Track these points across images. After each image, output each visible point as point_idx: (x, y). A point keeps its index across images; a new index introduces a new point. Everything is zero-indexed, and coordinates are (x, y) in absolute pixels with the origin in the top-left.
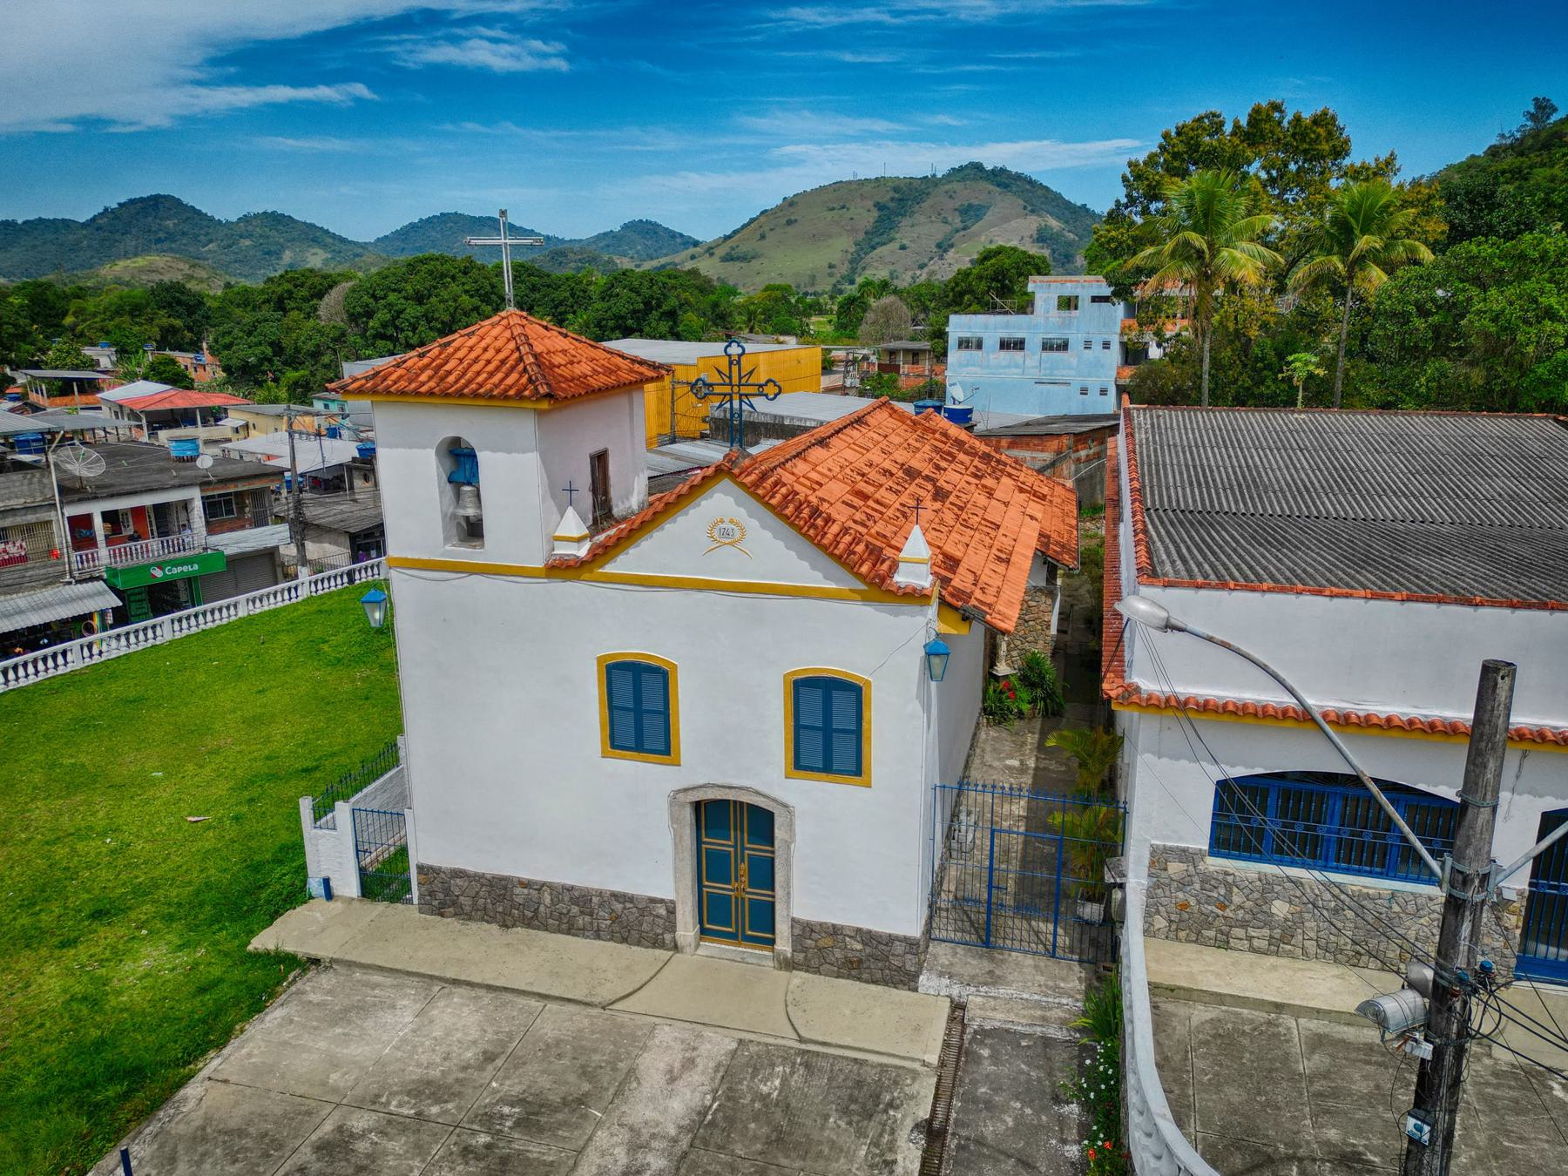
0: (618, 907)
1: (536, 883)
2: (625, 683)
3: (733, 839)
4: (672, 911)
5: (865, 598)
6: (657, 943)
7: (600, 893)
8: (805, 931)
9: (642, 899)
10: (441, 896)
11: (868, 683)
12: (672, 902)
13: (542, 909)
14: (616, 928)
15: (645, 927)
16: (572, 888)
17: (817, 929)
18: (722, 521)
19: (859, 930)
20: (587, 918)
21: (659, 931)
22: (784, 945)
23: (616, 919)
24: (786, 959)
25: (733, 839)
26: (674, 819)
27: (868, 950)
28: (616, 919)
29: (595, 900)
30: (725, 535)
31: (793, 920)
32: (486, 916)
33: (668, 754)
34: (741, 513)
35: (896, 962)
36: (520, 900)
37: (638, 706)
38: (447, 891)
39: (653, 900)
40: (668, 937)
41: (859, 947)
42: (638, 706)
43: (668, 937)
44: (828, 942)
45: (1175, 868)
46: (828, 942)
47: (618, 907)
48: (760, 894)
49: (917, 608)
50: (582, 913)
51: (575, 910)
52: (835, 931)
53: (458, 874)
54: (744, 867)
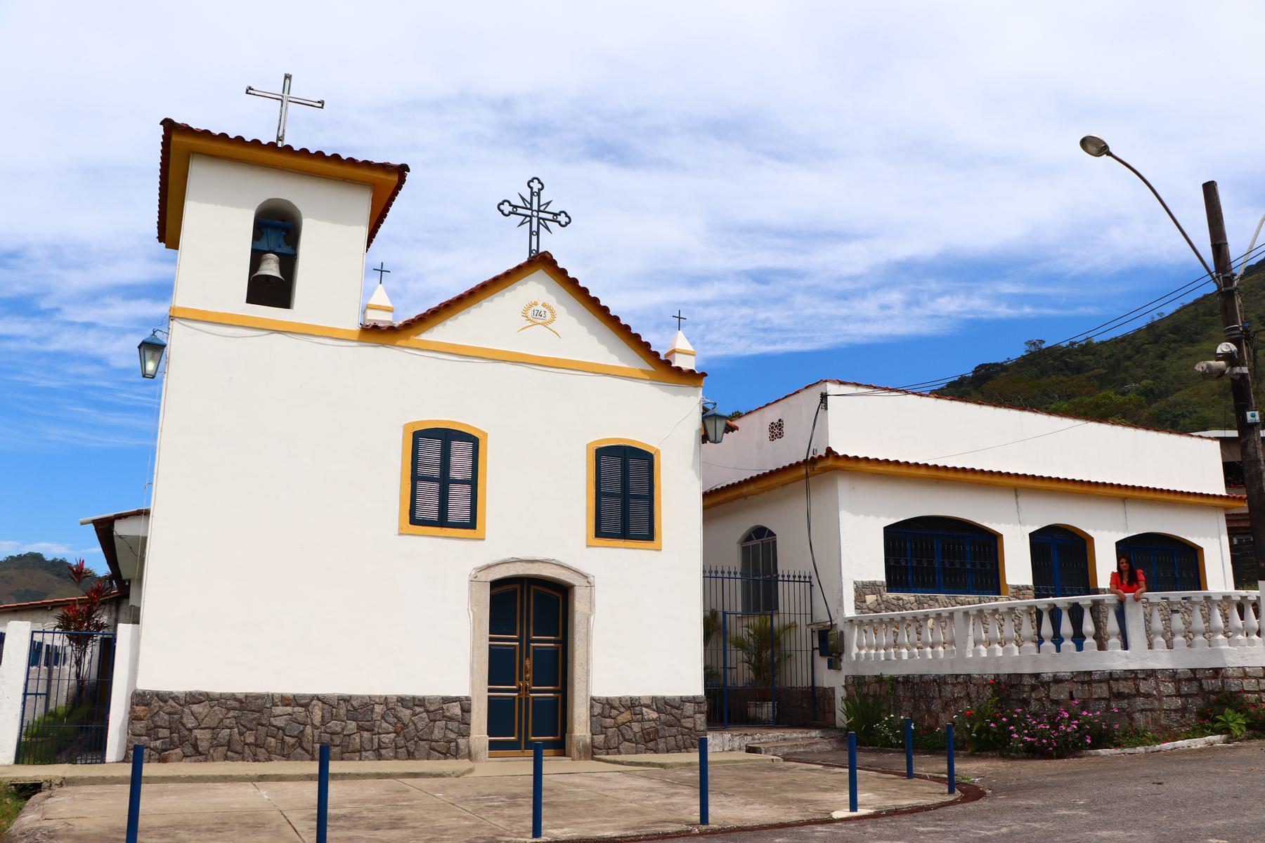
0: (405, 713)
1: (304, 697)
2: (432, 451)
3: (532, 613)
4: (466, 710)
5: (653, 379)
6: (450, 751)
7: (385, 700)
8: (605, 709)
9: (436, 698)
10: (164, 733)
11: (658, 451)
12: (468, 699)
13: (309, 729)
14: (401, 741)
15: (437, 734)
16: (346, 700)
17: (617, 704)
18: (536, 304)
19: (654, 699)
20: (366, 735)
21: (453, 736)
22: (581, 727)
23: (401, 729)
24: (585, 746)
25: (532, 613)
26: (473, 600)
27: (663, 717)
28: (401, 729)
29: (378, 709)
30: (536, 316)
31: (593, 699)
32: (232, 751)
33: (474, 528)
34: (552, 300)
35: (688, 723)
36: (279, 722)
37: (442, 480)
38: (175, 726)
39: (447, 700)
40: (461, 741)
41: (655, 715)
42: (442, 480)
43: (461, 741)
44: (626, 716)
45: (870, 599)
46: (626, 716)
47: (405, 713)
48: (545, 693)
49: (692, 389)
50: (360, 728)
51: (352, 725)
52: (633, 705)
53: (195, 698)
54: (528, 663)
